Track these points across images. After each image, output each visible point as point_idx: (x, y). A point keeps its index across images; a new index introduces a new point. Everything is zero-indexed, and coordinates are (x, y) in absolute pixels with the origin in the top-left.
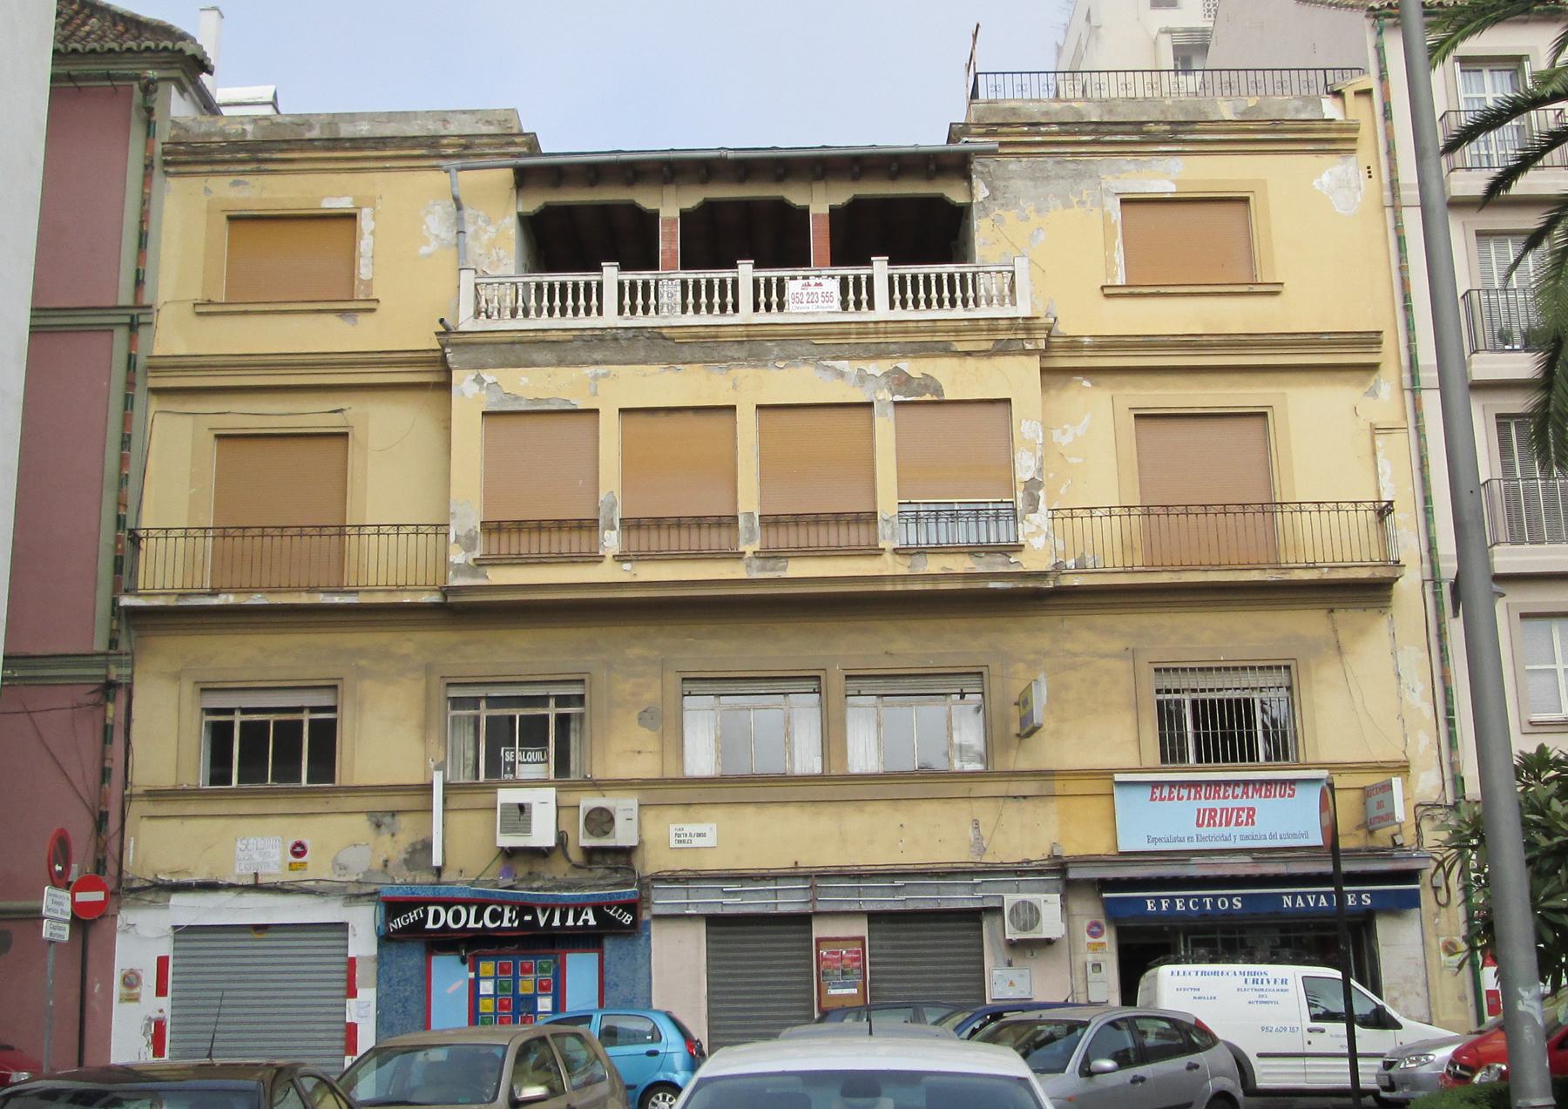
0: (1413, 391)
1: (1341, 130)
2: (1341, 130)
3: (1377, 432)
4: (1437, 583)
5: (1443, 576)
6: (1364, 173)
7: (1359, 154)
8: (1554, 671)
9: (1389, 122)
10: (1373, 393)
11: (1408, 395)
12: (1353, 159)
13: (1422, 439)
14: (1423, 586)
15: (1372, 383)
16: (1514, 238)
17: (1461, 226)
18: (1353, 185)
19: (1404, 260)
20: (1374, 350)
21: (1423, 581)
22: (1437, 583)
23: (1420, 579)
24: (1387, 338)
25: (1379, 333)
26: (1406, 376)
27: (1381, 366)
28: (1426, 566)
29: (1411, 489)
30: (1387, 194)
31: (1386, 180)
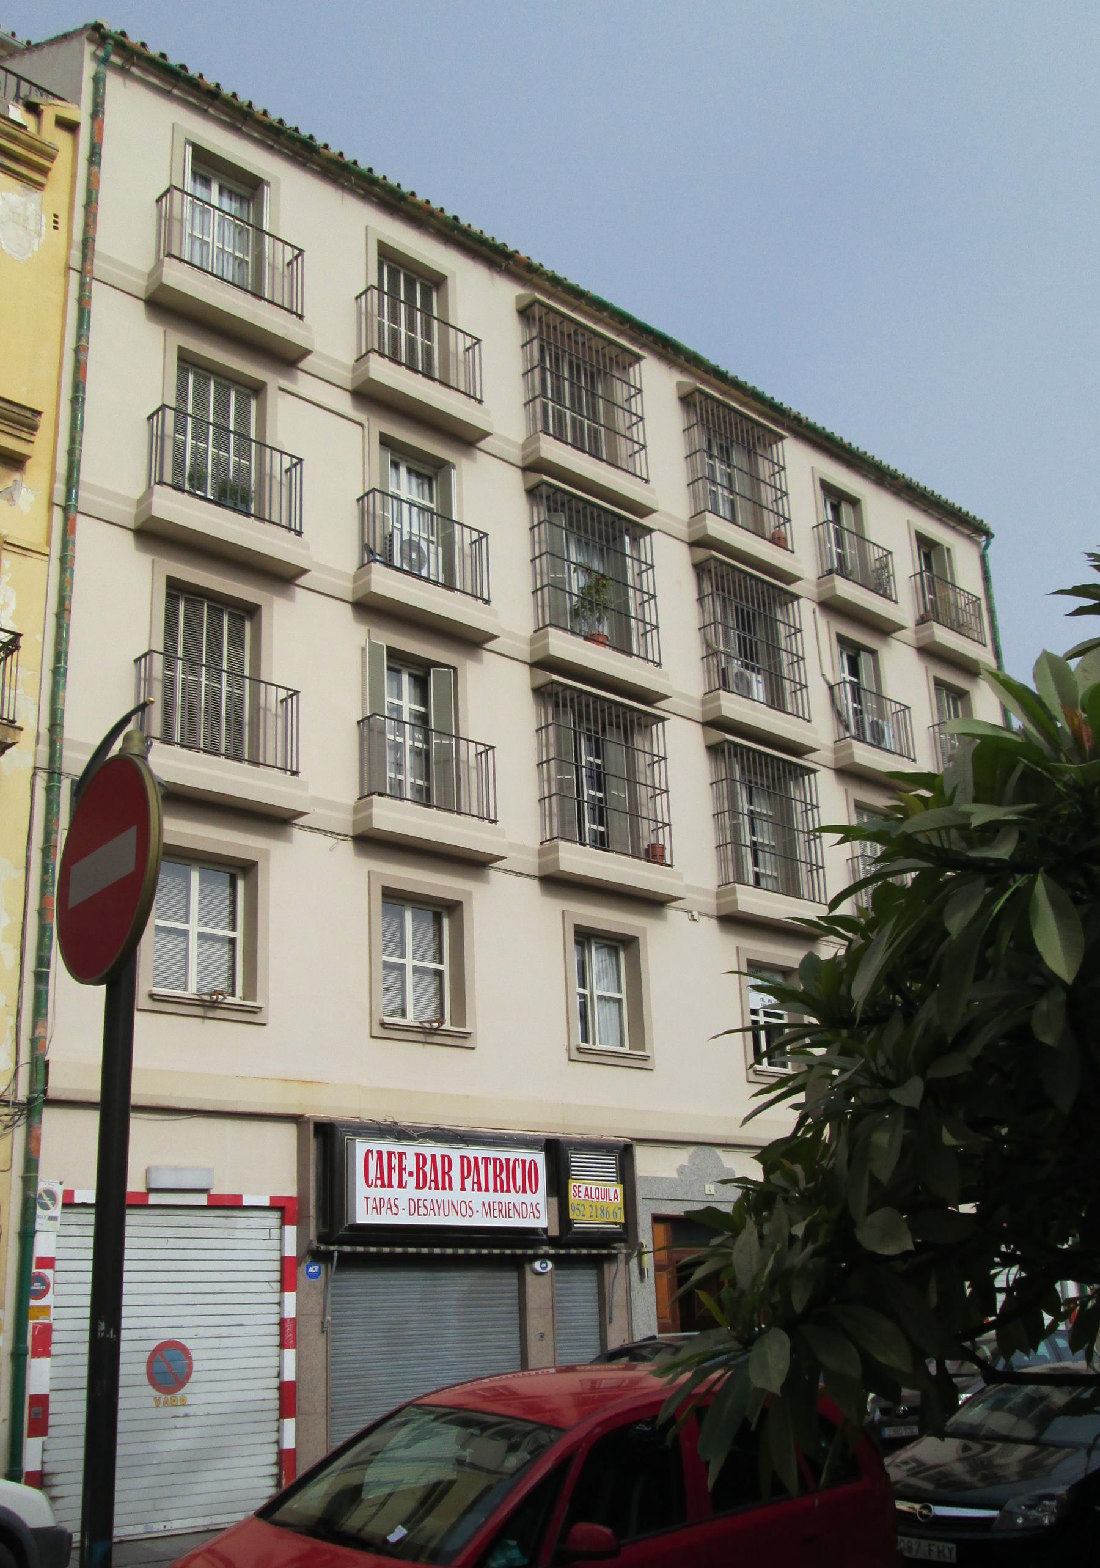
0: (66, 509)
1: (30, 148)
2: (30, 148)
3: (6, 546)
4: (54, 772)
5: (65, 768)
6: (47, 221)
7: (47, 193)
8: (185, 933)
9: (95, 169)
10: (10, 496)
11: (58, 513)
12: (36, 195)
13: (68, 574)
14: (34, 774)
15: (10, 483)
16: (219, 380)
17: (162, 334)
18: (31, 227)
19: (84, 339)
20: (24, 435)
21: (35, 768)
22: (54, 772)
23: (31, 764)
24: (45, 423)
25: (38, 413)
26: (60, 487)
27: (29, 463)
28: (44, 749)
29: (39, 637)
30: (76, 255)
31: (78, 236)
